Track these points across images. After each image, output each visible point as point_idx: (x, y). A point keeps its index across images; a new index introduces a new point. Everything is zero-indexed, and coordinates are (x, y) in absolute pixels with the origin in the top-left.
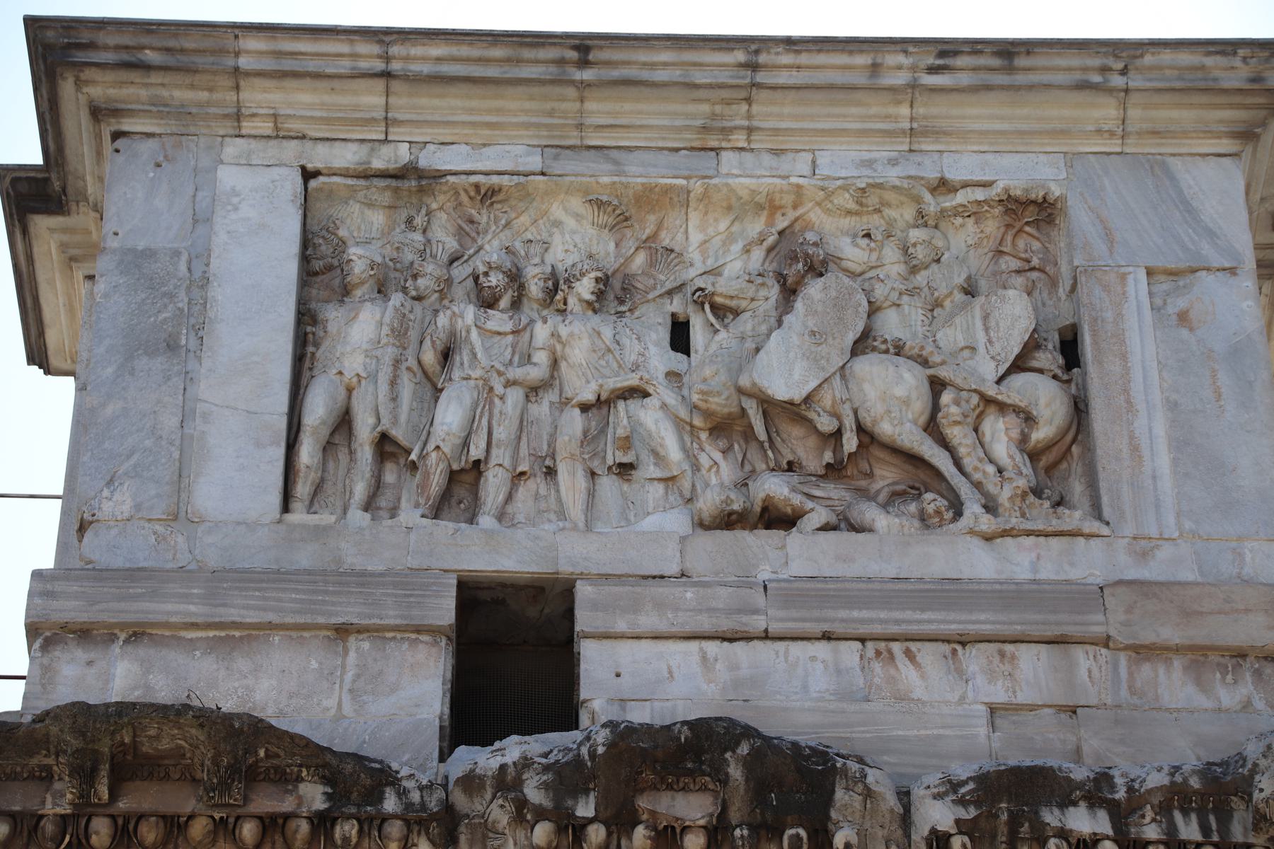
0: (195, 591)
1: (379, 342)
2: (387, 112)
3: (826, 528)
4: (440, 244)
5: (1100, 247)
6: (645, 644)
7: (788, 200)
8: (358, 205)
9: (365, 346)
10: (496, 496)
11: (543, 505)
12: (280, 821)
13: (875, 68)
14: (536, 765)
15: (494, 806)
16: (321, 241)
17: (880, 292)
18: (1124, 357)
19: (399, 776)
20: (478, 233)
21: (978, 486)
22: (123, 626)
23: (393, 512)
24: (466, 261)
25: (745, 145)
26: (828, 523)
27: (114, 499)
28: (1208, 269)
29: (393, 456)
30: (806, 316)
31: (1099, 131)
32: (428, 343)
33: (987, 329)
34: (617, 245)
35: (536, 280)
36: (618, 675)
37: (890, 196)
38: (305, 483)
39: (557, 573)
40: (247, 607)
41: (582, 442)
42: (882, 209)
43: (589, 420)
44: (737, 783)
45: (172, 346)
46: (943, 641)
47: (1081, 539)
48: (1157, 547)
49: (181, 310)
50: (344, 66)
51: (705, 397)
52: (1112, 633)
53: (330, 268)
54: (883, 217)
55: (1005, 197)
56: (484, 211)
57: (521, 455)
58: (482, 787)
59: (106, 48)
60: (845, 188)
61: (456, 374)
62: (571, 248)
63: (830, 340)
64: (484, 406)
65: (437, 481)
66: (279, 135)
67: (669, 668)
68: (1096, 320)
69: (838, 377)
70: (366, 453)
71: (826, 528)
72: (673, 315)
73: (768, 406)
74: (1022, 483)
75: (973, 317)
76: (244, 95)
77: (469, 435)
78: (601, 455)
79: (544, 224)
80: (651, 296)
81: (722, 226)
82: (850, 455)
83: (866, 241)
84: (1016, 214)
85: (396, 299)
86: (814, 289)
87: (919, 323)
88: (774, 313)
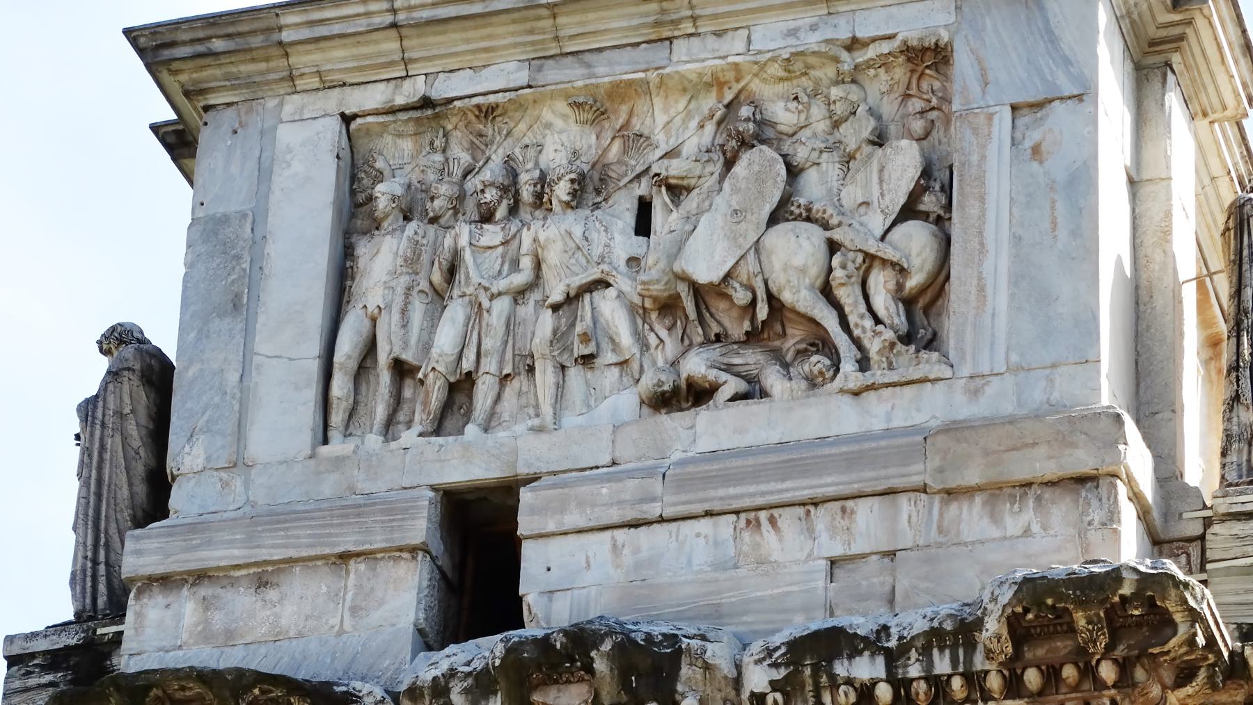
0: (238, 537)
2: (404, 53)
3: (736, 398)
4: (456, 161)
6: (571, 539)
7: (730, 75)
8: (391, 136)
9: (384, 278)
10: (485, 399)
11: (523, 401)
14: (459, 674)
16: (363, 175)
17: (801, 155)
18: (982, 199)
19: (361, 694)
20: (486, 145)
21: (857, 343)
22: (190, 573)
25: (693, 30)
27: (193, 453)
28: (1062, 99)
33: (881, 181)
34: (598, 137)
35: (527, 186)
37: (812, 60)
38: (337, 413)
39: (517, 476)
40: (274, 546)
41: (551, 342)
42: (808, 71)
43: (559, 318)
44: (603, 674)
46: (800, 505)
49: (244, 270)
50: (361, 25)
51: (647, 287)
55: (905, 48)
57: (507, 358)
58: (422, 696)
61: (456, 292)
62: (559, 147)
63: (749, 216)
64: (475, 320)
67: (587, 558)
70: (385, 377)
71: (736, 398)
73: (697, 290)
75: (871, 172)
76: (292, 60)
78: (567, 349)
79: (538, 127)
80: (621, 184)
83: (795, 104)
87: (835, 178)
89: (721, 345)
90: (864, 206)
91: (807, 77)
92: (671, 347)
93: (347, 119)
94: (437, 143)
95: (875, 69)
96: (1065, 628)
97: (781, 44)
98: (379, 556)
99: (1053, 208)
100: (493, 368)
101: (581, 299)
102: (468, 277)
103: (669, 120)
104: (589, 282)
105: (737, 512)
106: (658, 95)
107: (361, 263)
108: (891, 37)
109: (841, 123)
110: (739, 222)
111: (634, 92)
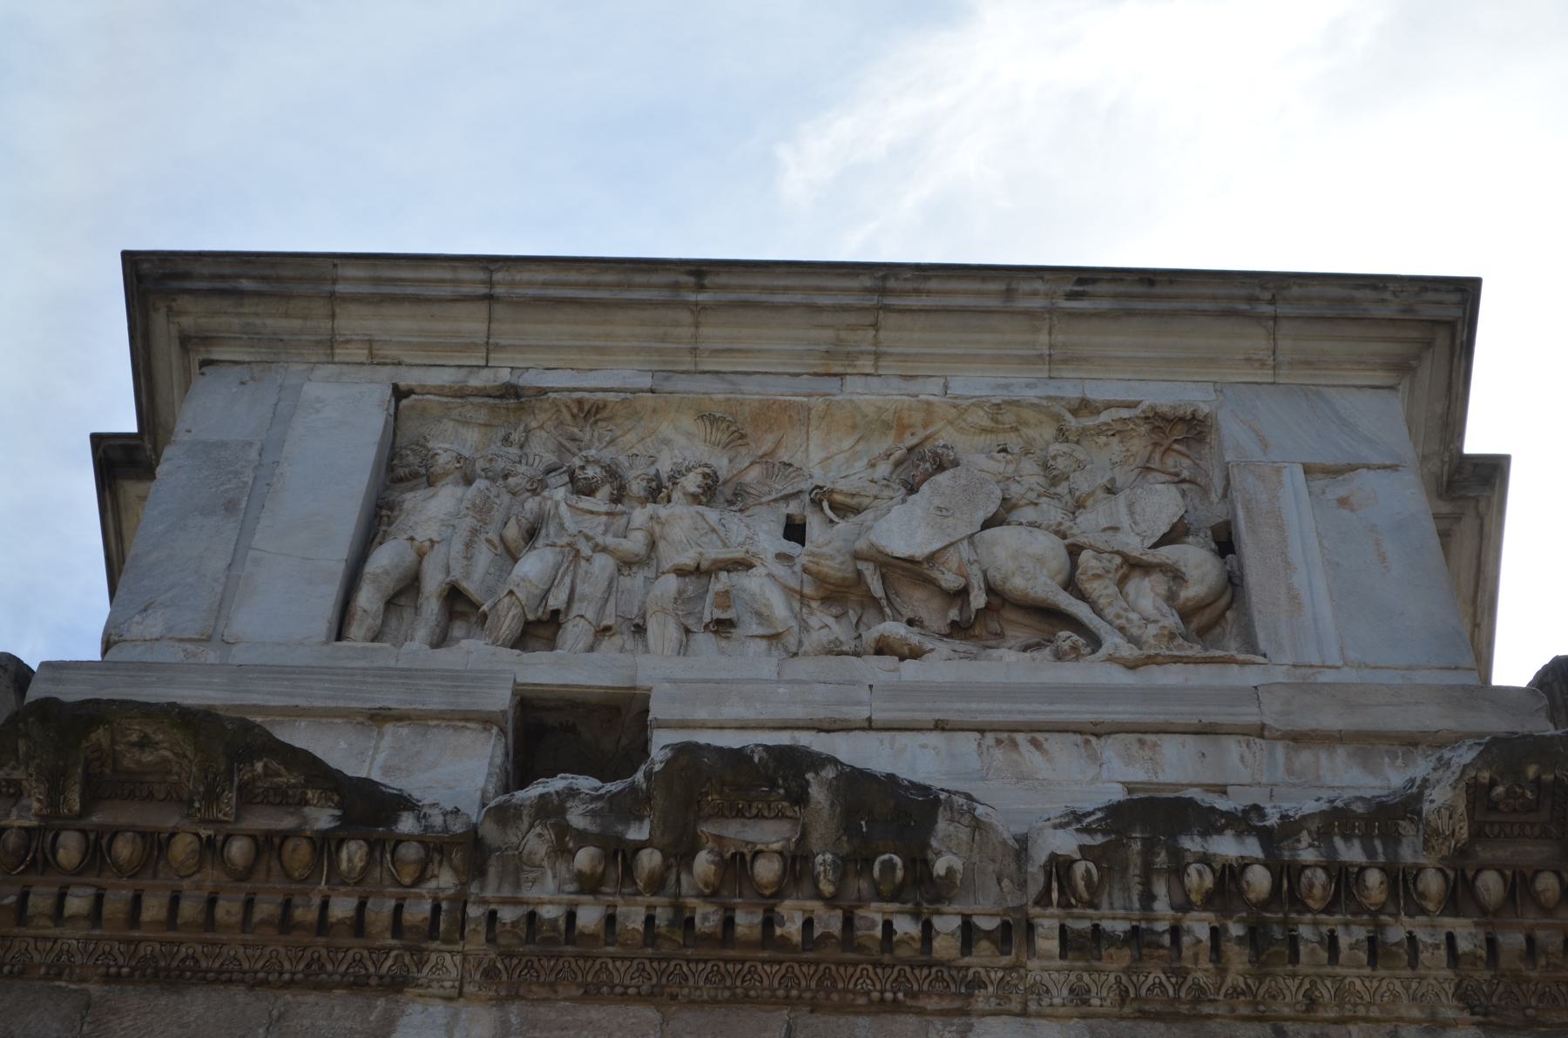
0: (216, 680)
2: (488, 338)
4: (537, 458)
8: (452, 423)
12: (277, 841)
13: (1009, 294)
14: (582, 796)
15: (531, 835)
16: (409, 452)
19: (420, 804)
25: (872, 371)
28: (1369, 467)
29: (463, 616)
31: (1248, 360)
32: (513, 521)
33: (1132, 513)
34: (730, 461)
35: (638, 480)
37: (1028, 415)
39: (634, 688)
41: (676, 599)
42: (1019, 427)
44: (819, 807)
45: (230, 507)
46: (1075, 732)
50: (446, 291)
51: (815, 559)
52: (1268, 721)
54: (1021, 436)
55: (1151, 415)
58: (518, 816)
59: (202, 277)
60: (979, 405)
64: (568, 567)
66: (375, 361)
72: (789, 517)
76: (341, 323)
77: (548, 591)
79: (652, 442)
80: (764, 499)
81: (846, 444)
82: (978, 611)
84: (1164, 433)
85: (480, 484)
91: (1017, 433)
96: (1537, 831)
98: (431, 723)
104: (729, 560)
106: (817, 428)
111: (787, 418)
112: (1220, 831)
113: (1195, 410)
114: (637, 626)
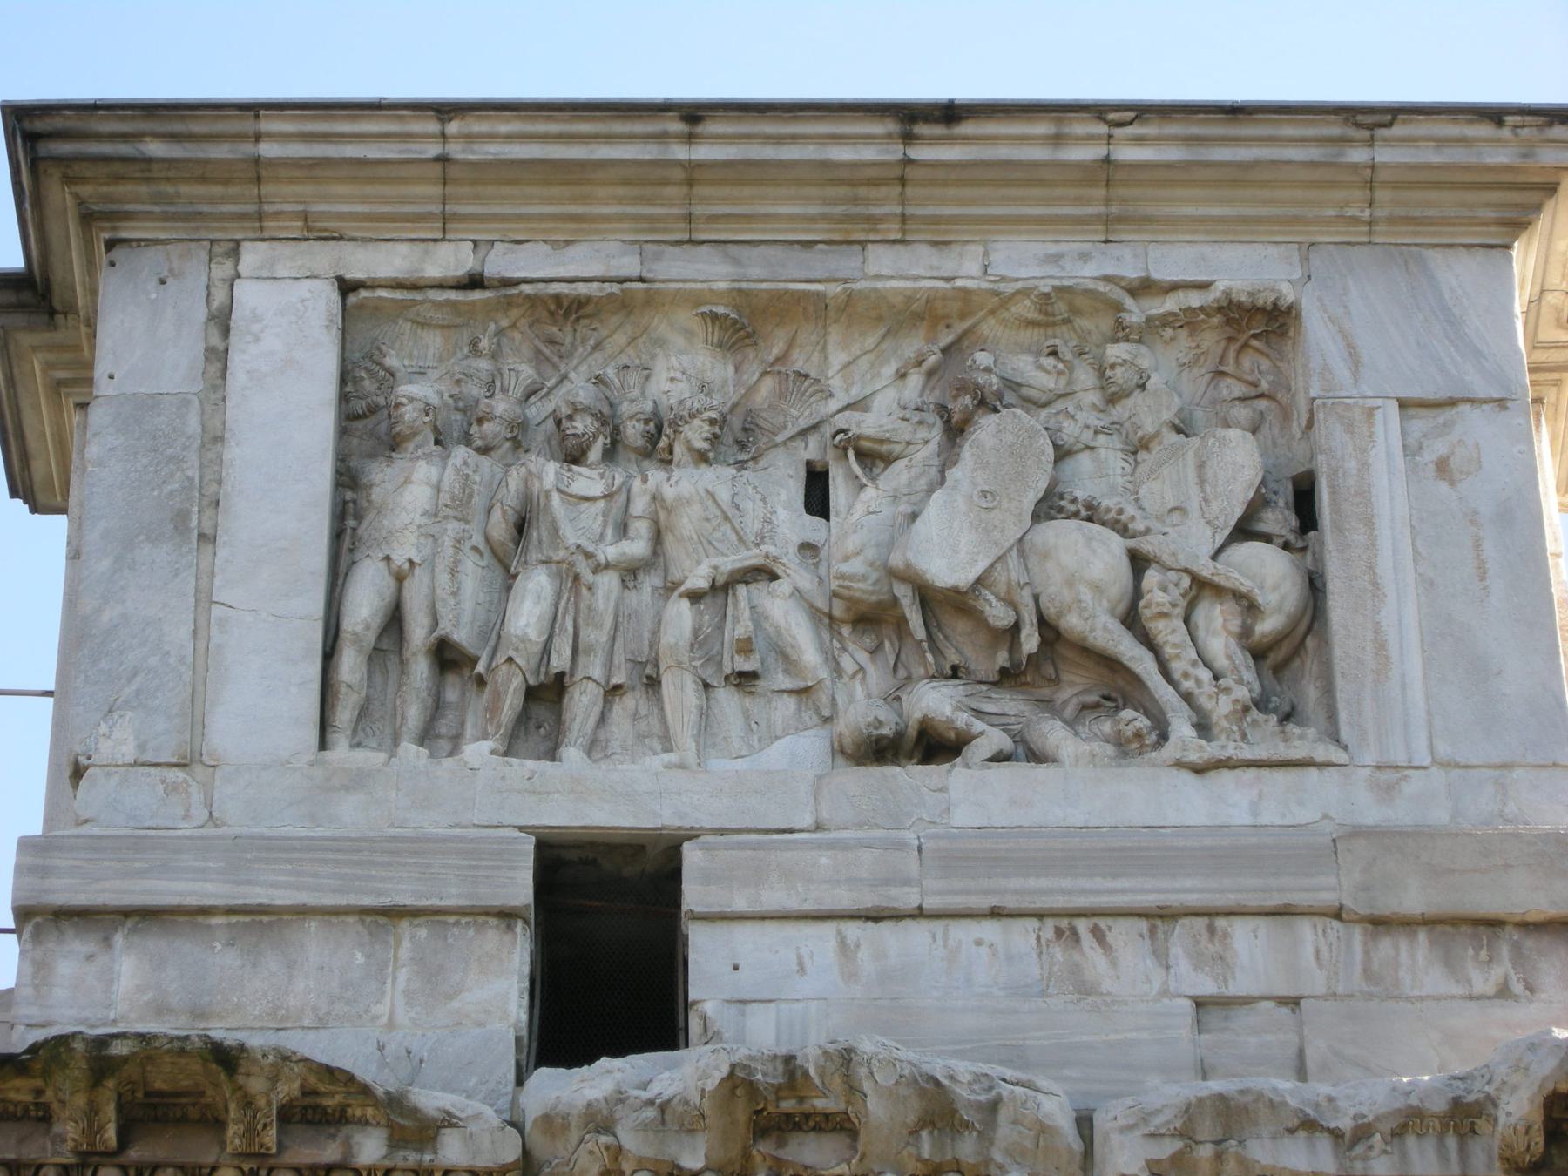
1: (436, 515)
3: (1000, 758)
5: (1342, 372)
6: (771, 928)
8: (409, 324)
9: (419, 520)
15: (582, 1151)
16: (363, 374)
18: (1369, 522)
23: (456, 742)
24: (546, 395)
26: (1001, 752)
27: (113, 737)
28: (1472, 401)
30: (976, 470)
33: (1202, 482)
34: (737, 370)
36: (736, 968)
37: (1080, 302)
40: (275, 885)
41: (692, 645)
43: (701, 613)
46: (1140, 915)
47: (1313, 771)
48: (1405, 778)
49: (190, 479)
51: (846, 583)
52: (1348, 902)
53: (373, 410)
54: (1074, 330)
55: (1225, 304)
56: (568, 329)
57: (616, 662)
58: (566, 1127)
61: (534, 555)
62: (678, 375)
63: (1005, 504)
64: (569, 600)
65: (512, 701)
68: (1335, 472)
69: (1014, 553)
70: (421, 668)
72: (809, 463)
73: (928, 597)
74: (1242, 693)
75: (1185, 466)
80: (779, 439)
82: (1030, 656)
83: (1051, 361)
84: (1239, 324)
86: (986, 429)
87: (1119, 471)
88: (936, 462)
89: (957, 682)
90: (1178, 512)
91: (1069, 326)
92: (877, 677)
93: (347, 287)
94: (484, 343)
95: (1174, 328)
97: (1038, 272)
98: (452, 919)
99: (1477, 547)
100: (597, 672)
101: (730, 592)
102: (555, 531)
103: (851, 359)
104: (746, 568)
105: (1040, 915)
106: (836, 321)
107: (376, 494)
108: (1204, 286)
109: (1120, 398)
110: (993, 509)
111: (801, 309)
112: (1291, 1131)
113: (1277, 299)
114: (649, 677)
